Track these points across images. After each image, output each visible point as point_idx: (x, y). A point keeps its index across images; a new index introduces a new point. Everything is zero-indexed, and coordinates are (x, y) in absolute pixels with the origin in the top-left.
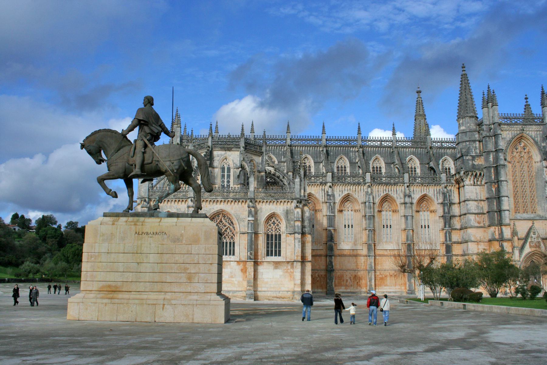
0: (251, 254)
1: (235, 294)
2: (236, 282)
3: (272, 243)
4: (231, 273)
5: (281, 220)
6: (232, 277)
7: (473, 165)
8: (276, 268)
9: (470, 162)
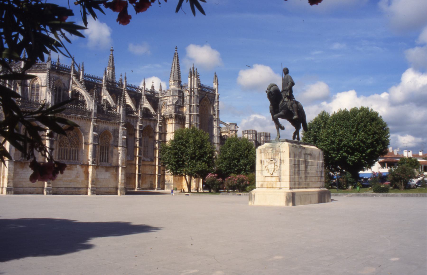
0: (94, 160)
1: (80, 190)
2: (80, 181)
3: (103, 153)
4: (77, 174)
5: (110, 136)
6: (77, 177)
7: (179, 111)
8: (107, 171)
9: (178, 109)
